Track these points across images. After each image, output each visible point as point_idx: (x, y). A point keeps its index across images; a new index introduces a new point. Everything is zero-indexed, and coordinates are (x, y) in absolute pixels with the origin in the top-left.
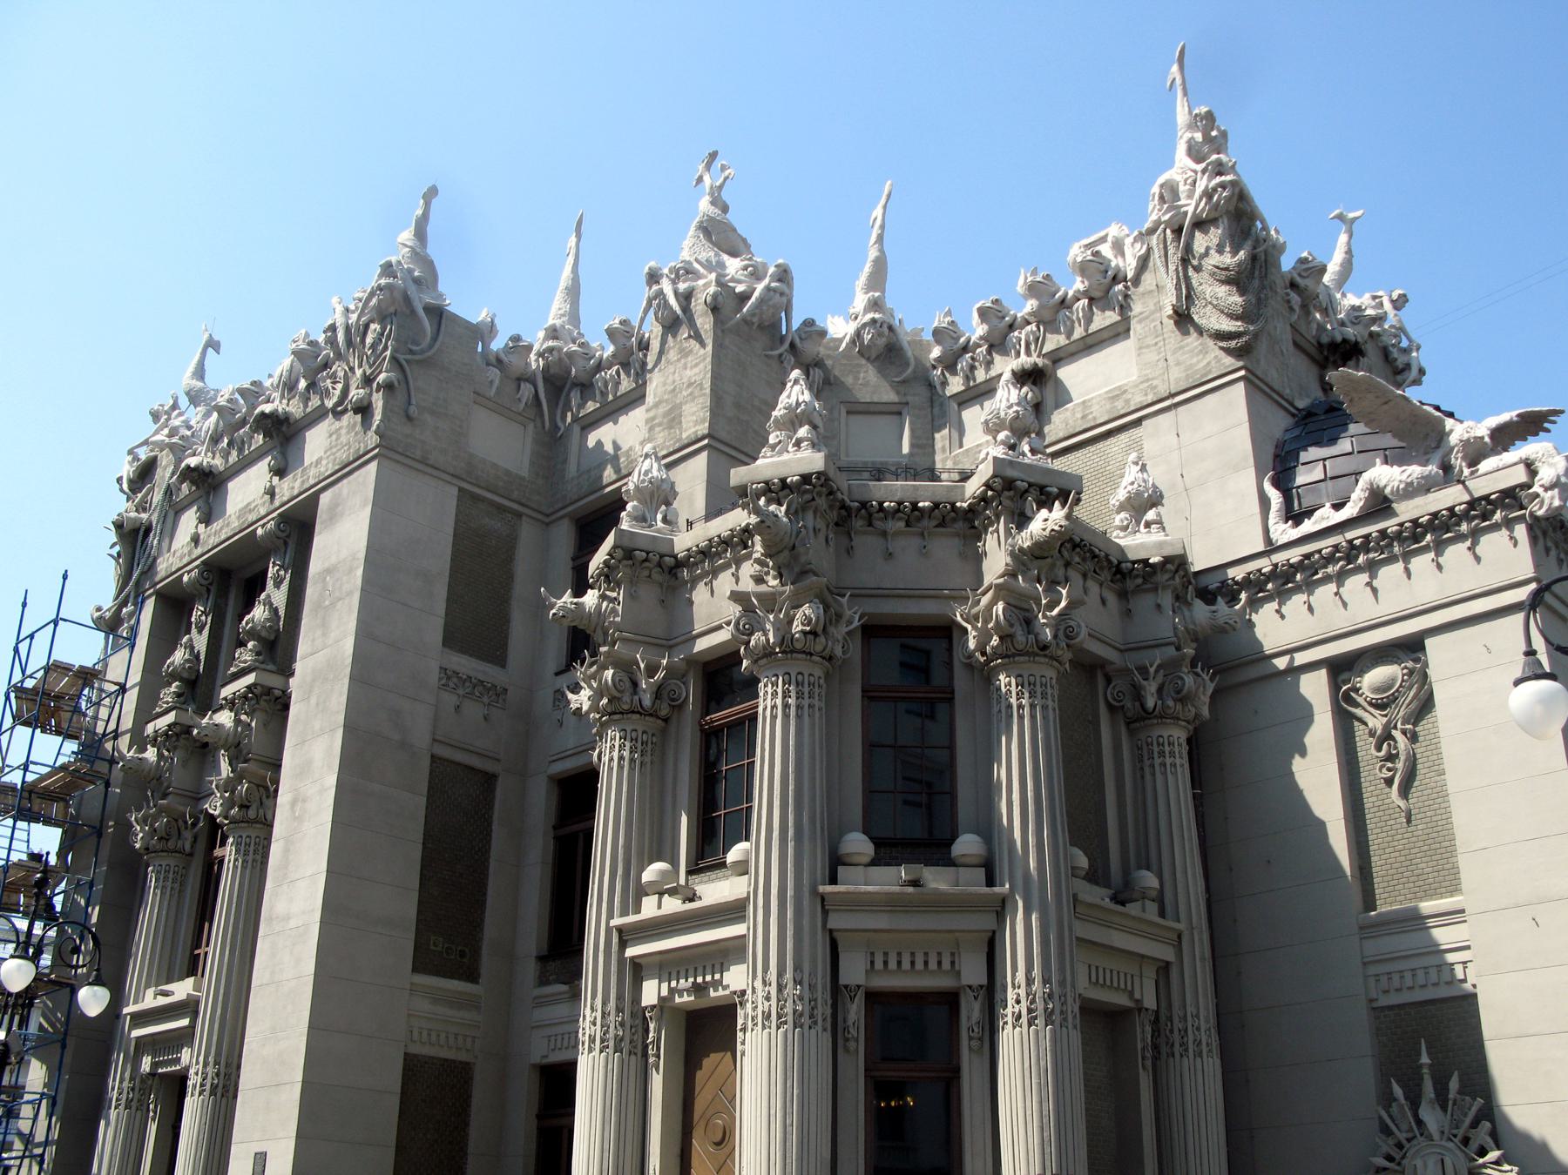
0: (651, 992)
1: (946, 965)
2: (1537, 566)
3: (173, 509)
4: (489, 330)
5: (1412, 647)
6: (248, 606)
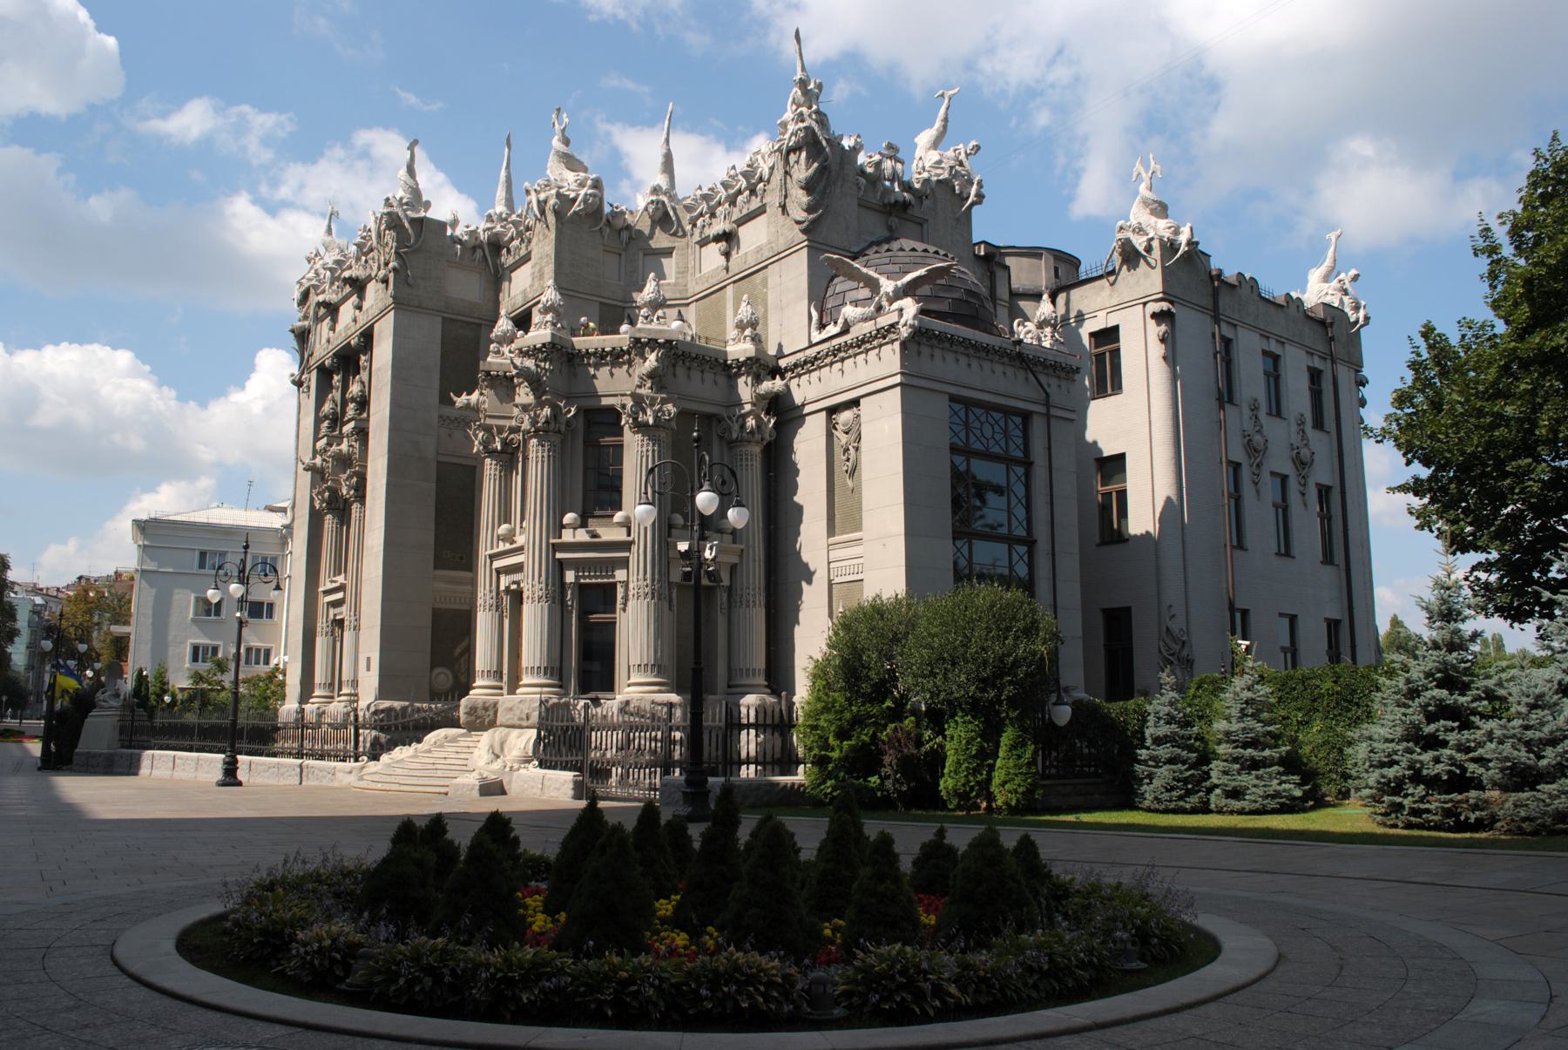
2: (902, 366)
3: (318, 320)
5: (855, 403)
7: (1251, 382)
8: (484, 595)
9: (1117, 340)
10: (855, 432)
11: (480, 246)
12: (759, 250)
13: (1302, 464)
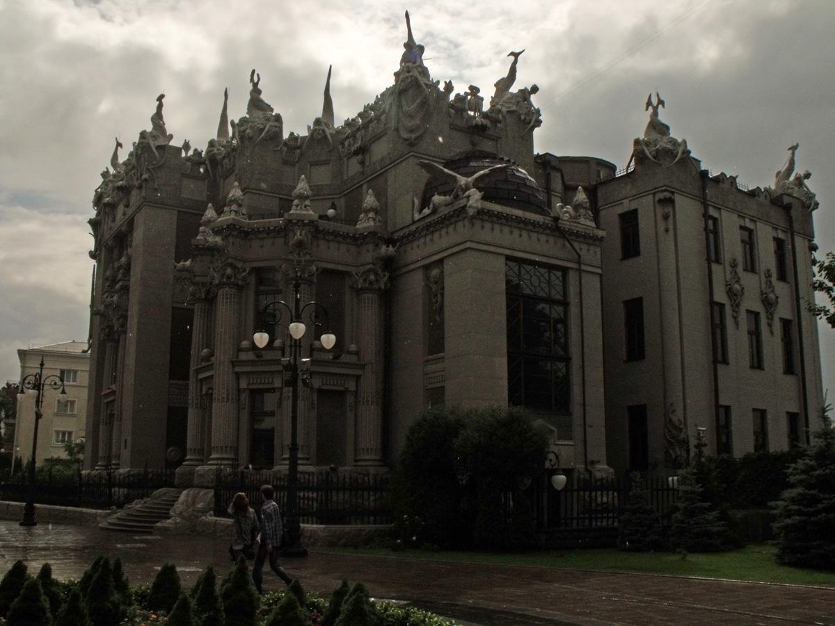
0: (243, 384)
1: (270, 381)
4: (187, 146)
6: (120, 256)
7: (732, 245)
9: (636, 219)
10: (440, 281)
11: (204, 163)
12: (382, 159)
13: (769, 304)
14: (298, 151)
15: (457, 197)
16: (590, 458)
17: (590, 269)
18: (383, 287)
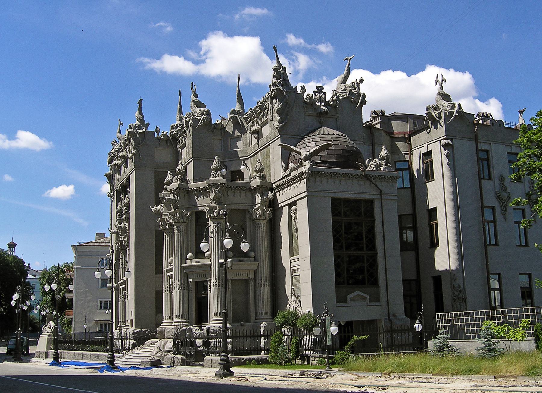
4: (158, 131)
8: (165, 287)
14: (222, 131)
15: (301, 164)
16: (391, 313)
17: (388, 197)
18: (267, 216)
